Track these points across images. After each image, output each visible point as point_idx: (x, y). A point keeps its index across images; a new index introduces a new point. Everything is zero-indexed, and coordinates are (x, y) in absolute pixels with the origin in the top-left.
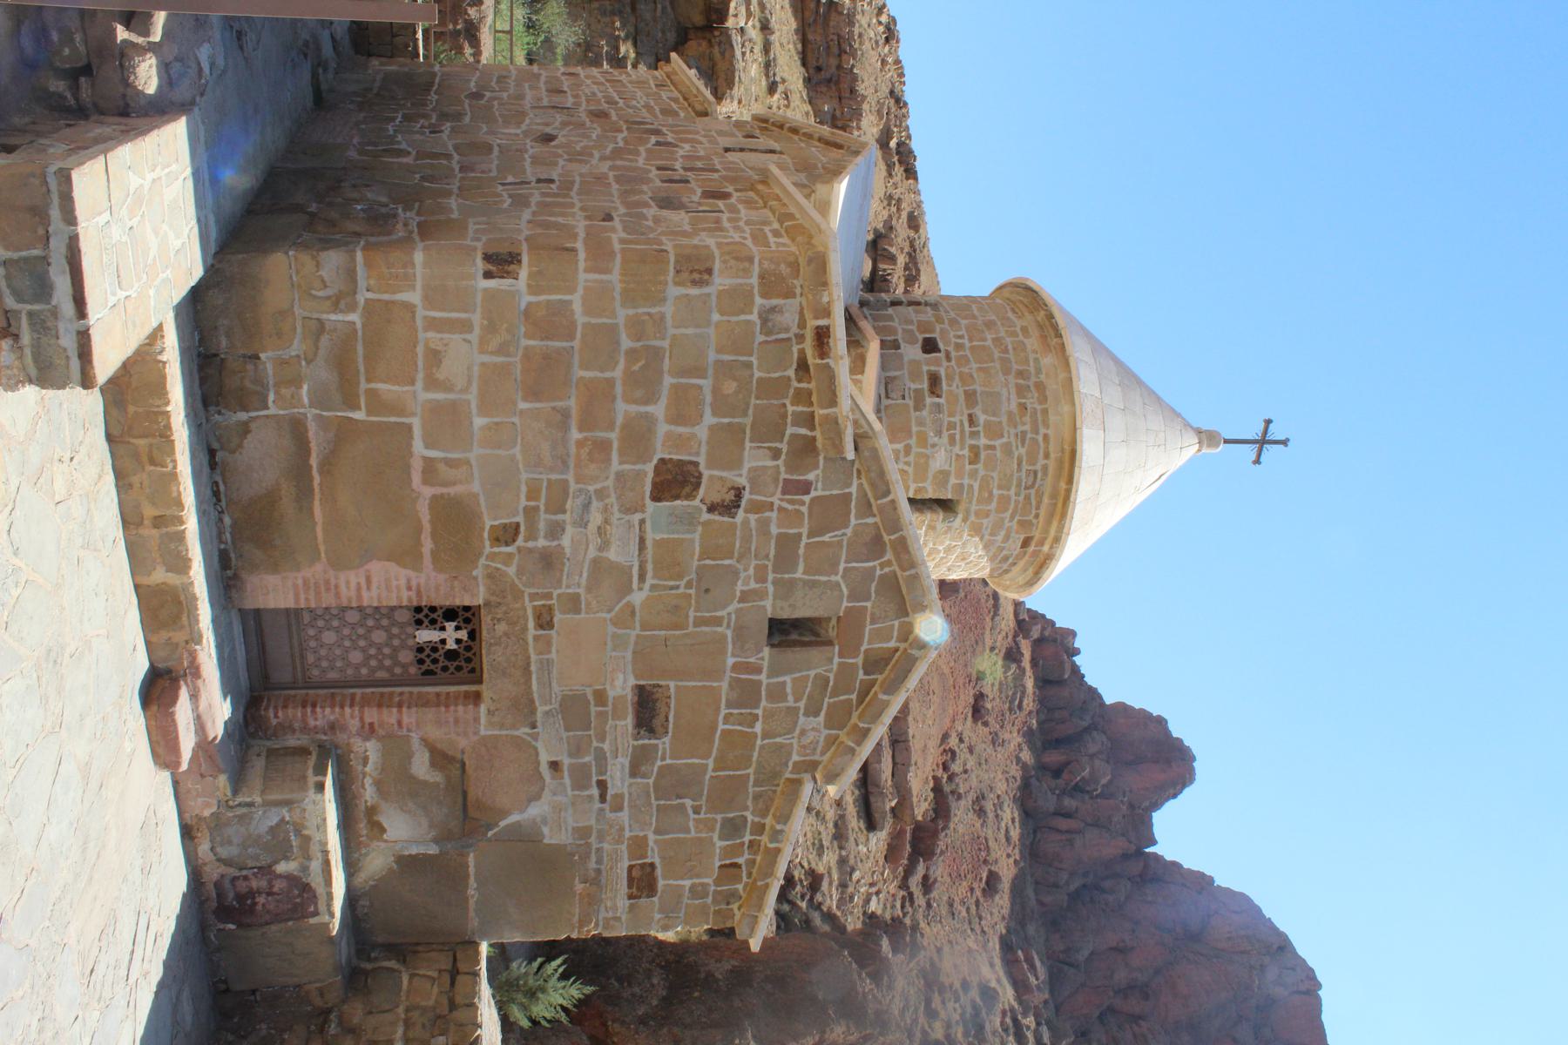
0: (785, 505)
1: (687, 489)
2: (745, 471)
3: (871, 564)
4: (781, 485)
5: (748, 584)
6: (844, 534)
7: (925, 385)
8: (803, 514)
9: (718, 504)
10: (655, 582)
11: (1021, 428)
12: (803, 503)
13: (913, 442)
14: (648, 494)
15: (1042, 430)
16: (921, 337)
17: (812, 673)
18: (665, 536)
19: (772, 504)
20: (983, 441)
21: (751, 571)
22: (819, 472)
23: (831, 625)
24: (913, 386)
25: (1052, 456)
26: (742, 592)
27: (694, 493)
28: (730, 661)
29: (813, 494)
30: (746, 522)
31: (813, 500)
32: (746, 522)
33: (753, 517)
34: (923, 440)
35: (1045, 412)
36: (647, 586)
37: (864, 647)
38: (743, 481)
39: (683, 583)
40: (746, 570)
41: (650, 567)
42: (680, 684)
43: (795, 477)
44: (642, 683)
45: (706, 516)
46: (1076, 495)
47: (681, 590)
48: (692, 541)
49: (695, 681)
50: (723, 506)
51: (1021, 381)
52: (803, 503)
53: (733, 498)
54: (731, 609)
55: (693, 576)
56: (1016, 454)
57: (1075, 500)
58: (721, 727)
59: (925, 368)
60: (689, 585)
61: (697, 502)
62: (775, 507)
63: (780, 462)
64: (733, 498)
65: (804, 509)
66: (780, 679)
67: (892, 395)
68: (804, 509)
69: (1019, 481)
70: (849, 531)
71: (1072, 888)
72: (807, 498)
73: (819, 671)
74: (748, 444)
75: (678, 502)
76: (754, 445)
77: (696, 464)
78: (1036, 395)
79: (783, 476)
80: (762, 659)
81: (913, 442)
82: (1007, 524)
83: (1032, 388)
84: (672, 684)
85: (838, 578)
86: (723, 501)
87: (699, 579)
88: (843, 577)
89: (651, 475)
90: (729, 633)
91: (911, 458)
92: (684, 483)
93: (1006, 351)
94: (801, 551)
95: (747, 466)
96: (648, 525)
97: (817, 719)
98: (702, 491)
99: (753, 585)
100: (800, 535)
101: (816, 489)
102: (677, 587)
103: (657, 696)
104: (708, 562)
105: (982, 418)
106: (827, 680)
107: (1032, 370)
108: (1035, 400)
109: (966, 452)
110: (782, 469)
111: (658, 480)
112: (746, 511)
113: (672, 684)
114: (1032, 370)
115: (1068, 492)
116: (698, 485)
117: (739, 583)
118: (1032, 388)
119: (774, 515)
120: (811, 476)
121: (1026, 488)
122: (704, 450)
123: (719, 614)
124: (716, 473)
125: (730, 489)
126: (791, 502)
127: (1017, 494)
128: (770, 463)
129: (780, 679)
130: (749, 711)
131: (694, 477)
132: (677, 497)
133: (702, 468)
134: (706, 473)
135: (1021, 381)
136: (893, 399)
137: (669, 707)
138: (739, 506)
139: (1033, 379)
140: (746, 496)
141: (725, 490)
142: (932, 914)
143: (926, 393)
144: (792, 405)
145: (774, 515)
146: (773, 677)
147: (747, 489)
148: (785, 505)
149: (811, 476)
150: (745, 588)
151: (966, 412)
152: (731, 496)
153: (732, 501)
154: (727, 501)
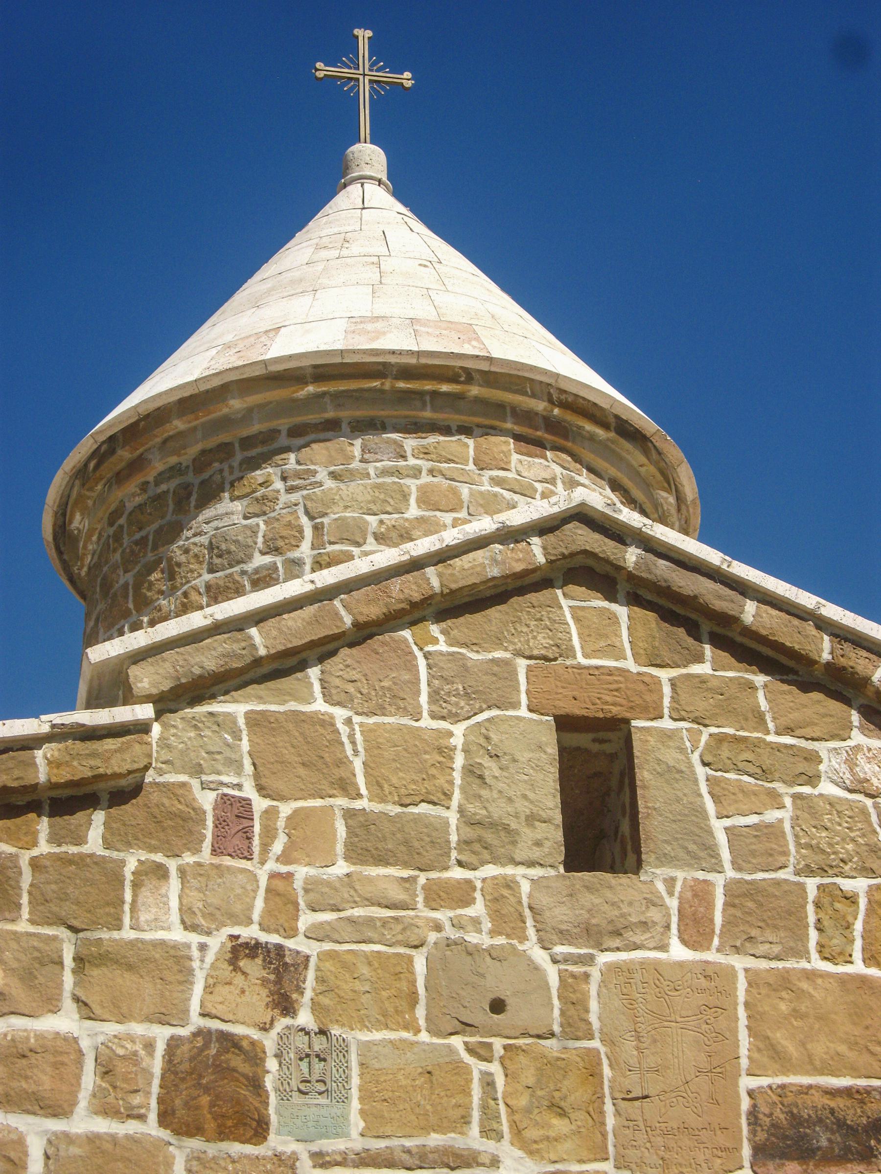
0: (278, 847)
1: (237, 1062)
2: (194, 939)
3: (422, 663)
4: (227, 861)
5: (476, 922)
6: (349, 721)
8: (296, 812)
9: (272, 993)
10: (475, 1129)
11: (279, 485)
12: (270, 814)
14: (249, 1149)
15: (283, 441)
17: (701, 772)
18: (355, 1104)
19: (273, 876)
21: (442, 916)
22: (195, 783)
23: (595, 747)
25: (330, 414)
26: (493, 933)
27: (245, 1044)
28: (678, 952)
29: (249, 791)
30: (317, 934)
31: (261, 789)
32: (317, 934)
33: (306, 920)
35: (247, 442)
36: (488, 1146)
37: (630, 664)
38: (217, 942)
39: (477, 1066)
40: (438, 928)
41: (435, 1140)
42: (744, 1062)
43: (209, 833)
44: (746, 1151)
45: (305, 1018)
46: (400, 353)
47: (495, 1068)
48: (366, 1047)
49: (735, 1032)
50: (279, 981)
52: (270, 814)
53: (259, 961)
54: (540, 956)
55: (457, 1042)
56: (329, 484)
57: (411, 353)
58: (858, 967)
60: (481, 1052)
61: (270, 1042)
62: (284, 869)
63: (172, 865)
64: (259, 961)
65: (286, 809)
66: (722, 839)
68: (286, 809)
69: (385, 472)
70: (340, 713)
72: (260, 804)
73: (695, 758)
74: (128, 934)
75: (269, 1082)
76: (127, 920)
77: (173, 1044)
78: (216, 465)
79: (205, 855)
80: (670, 882)
82: (486, 487)
83: (205, 475)
84: (747, 1082)
85: (459, 730)
86: (264, 982)
87: (466, 1026)
88: (456, 718)
89: (195, 1144)
90: (604, 958)
92: (224, 1071)
93: (142, 542)
94: (394, 810)
95: (177, 935)
96: (333, 1145)
97: (824, 754)
98: (238, 1030)
99: (478, 909)
100: (349, 814)
101: (239, 786)
102: (488, 1083)
103: (780, 1115)
104: (421, 1012)
106: (719, 740)
107: (172, 485)
108: (225, 466)
110: (189, 858)
111: (210, 1126)
112: (292, 933)
113: (747, 1082)
114: (172, 485)
115: (407, 372)
116: (229, 1042)
117: (473, 938)
118: (205, 475)
119: (302, 872)
120: (207, 800)
121: (404, 457)
122: (138, 1029)
123: (554, 980)
124: (195, 1006)
125: (236, 969)
126: (269, 835)
127: (416, 473)
128: (174, 884)
129: (722, 839)
130: (810, 909)
131: (206, 1046)
132: (256, 1085)
133: (184, 1032)
134: (196, 1021)
137: (810, 1087)
138: (280, 948)
139: (190, 477)
140: (251, 932)
141: (239, 979)
144: (35, 844)
145: (302, 872)
146: (716, 856)
147: (236, 931)
148: (278, 847)
149: (207, 800)
150: (487, 925)
152: (254, 968)
153: (267, 963)
154: (264, 973)
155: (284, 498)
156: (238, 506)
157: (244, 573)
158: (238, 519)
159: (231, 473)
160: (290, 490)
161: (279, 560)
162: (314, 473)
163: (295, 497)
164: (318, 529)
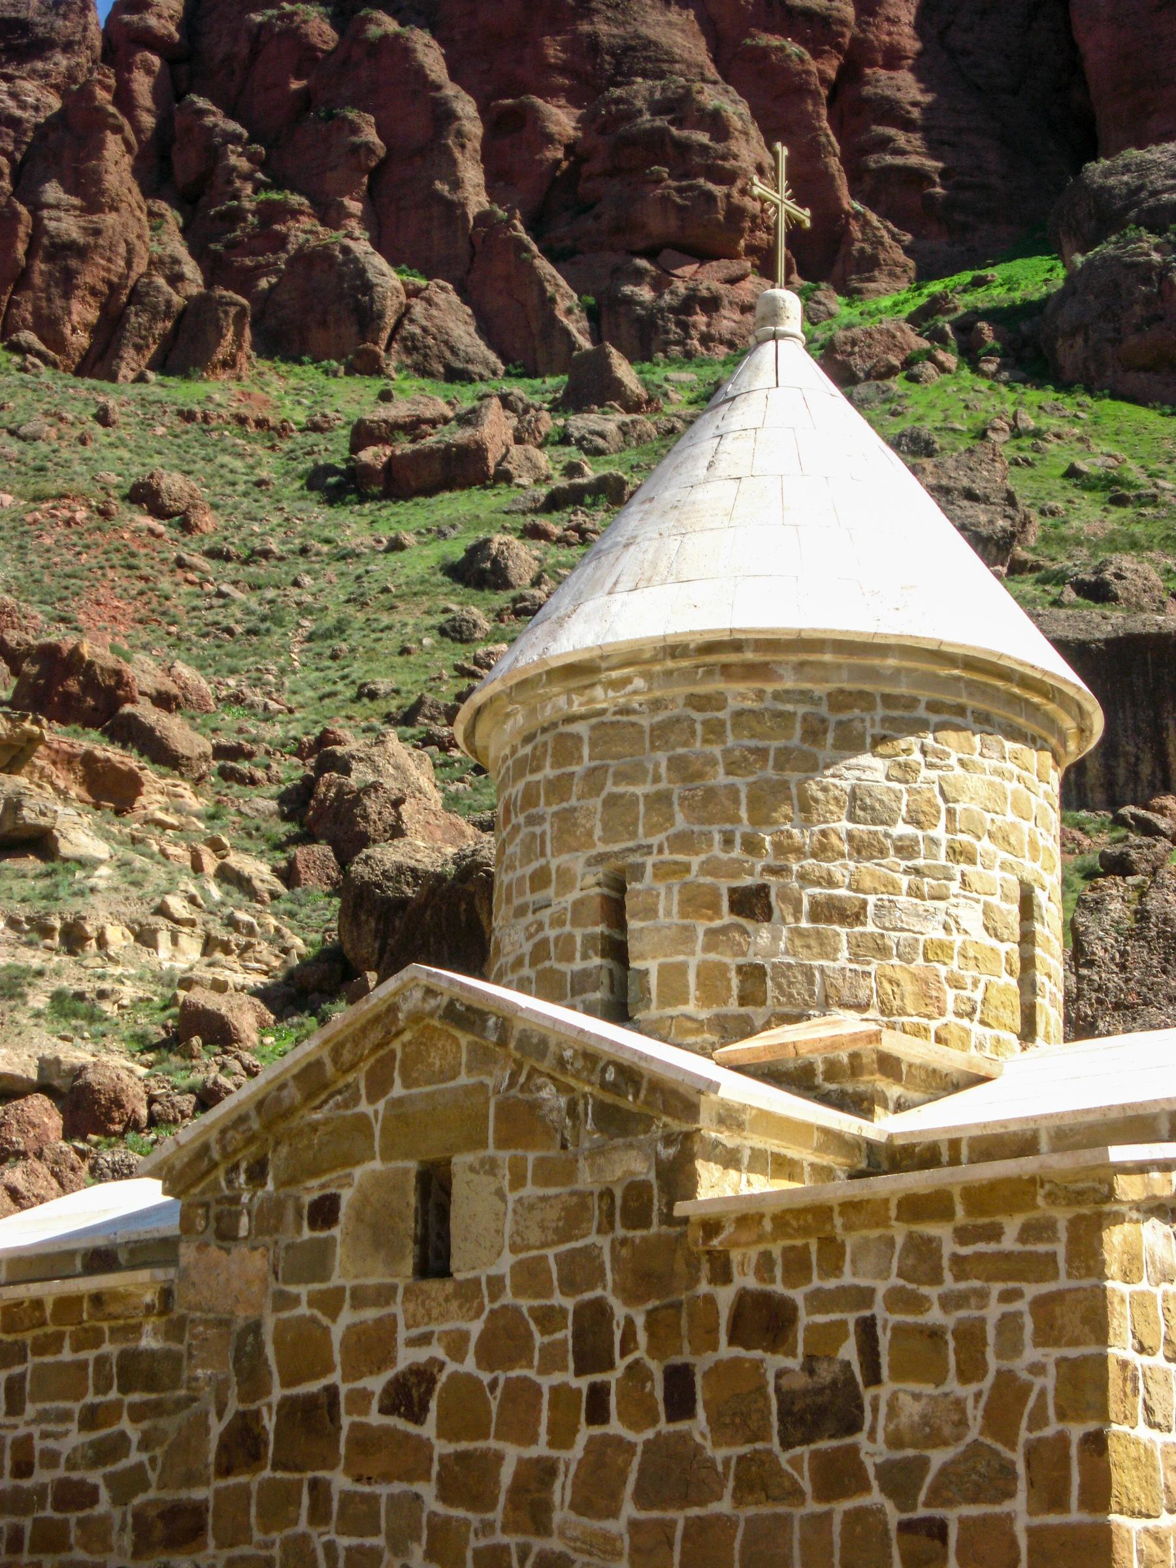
7: (843, 931)
11: (917, 756)
13: (943, 971)
15: (921, 712)
16: (727, 918)
20: (939, 832)
24: (844, 954)
34: (937, 951)
35: (889, 700)
51: (830, 738)
56: (959, 770)
59: (804, 924)
67: (863, 994)
71: (190, 269)
78: (857, 711)
81: (943, 971)
83: (844, 716)
91: (968, 975)
105: (901, 829)
107: (801, 709)
109: (957, 869)
114: (801, 709)
118: (844, 716)
135: (830, 738)
136: (871, 996)
139: (824, 710)
142: (256, 696)
143: (858, 929)
151: (892, 859)
155: (924, 773)
156: (877, 763)
157: (887, 835)
158: (880, 776)
159: (873, 726)
160: (930, 766)
161: (920, 834)
162: (948, 755)
163: (934, 774)
164: (951, 813)
